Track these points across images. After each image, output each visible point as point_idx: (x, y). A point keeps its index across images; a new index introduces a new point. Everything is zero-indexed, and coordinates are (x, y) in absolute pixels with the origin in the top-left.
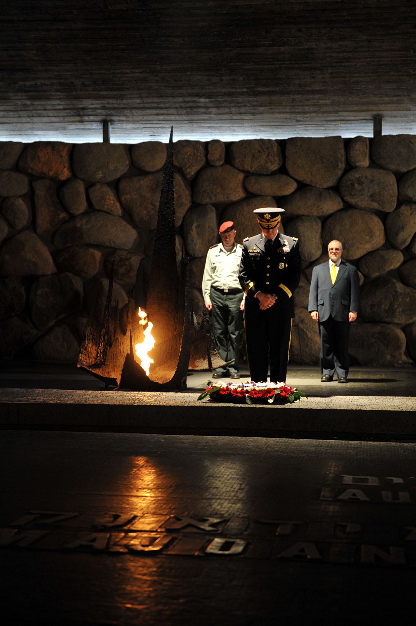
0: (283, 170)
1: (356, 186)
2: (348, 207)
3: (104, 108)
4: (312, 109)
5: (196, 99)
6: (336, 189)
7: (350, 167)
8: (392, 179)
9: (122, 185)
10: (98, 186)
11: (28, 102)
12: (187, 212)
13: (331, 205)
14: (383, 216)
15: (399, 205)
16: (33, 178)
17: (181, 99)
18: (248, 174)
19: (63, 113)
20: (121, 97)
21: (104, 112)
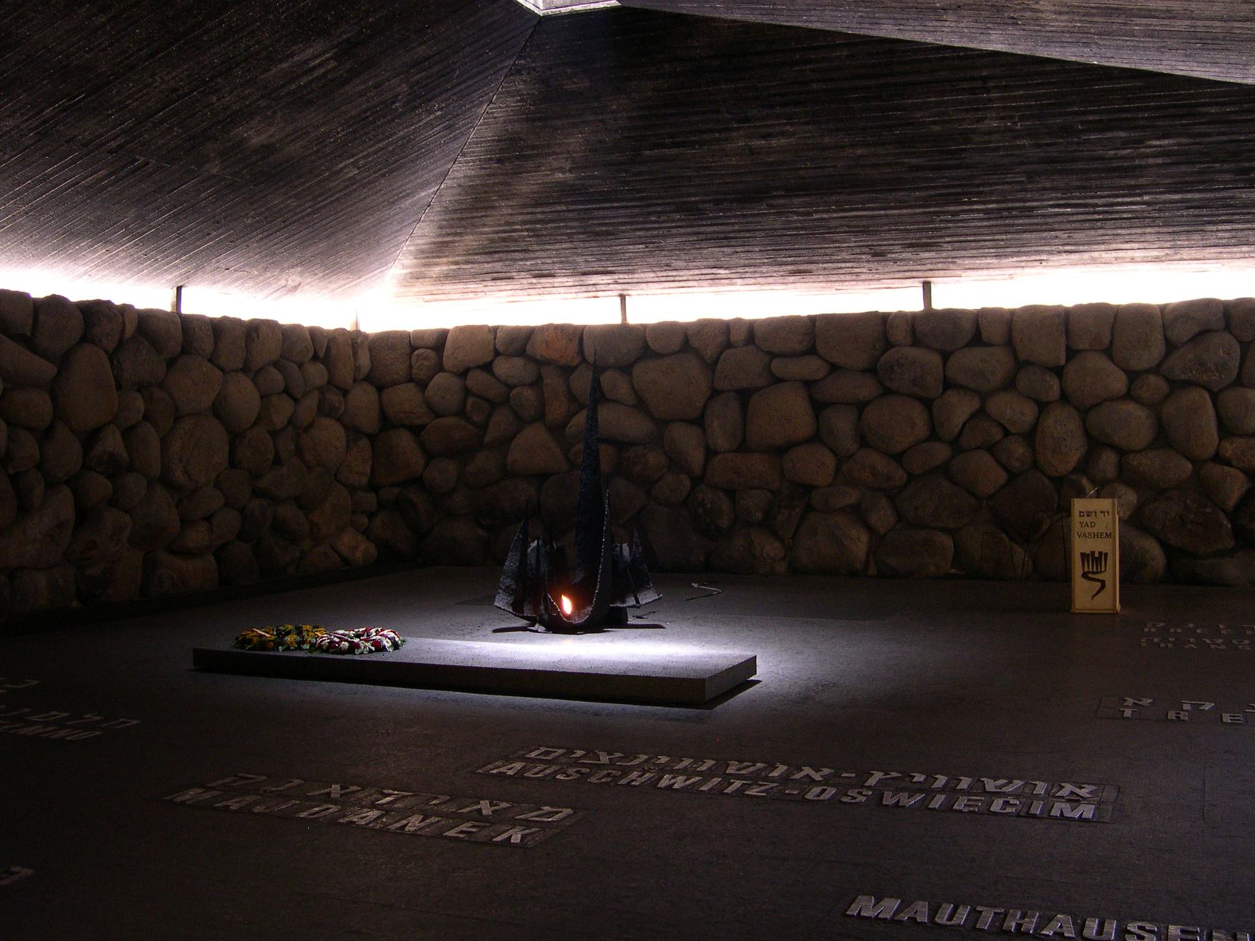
0: (812, 351)
1: (896, 368)
2: (887, 392)
3: (616, 283)
4: (848, 277)
5: (714, 271)
6: (871, 370)
7: (888, 345)
8: (936, 359)
9: (638, 370)
10: (609, 373)
11: (534, 281)
12: (709, 399)
13: (865, 388)
14: (927, 403)
15: (945, 390)
16: (540, 363)
17: (697, 272)
18: (773, 355)
19: (574, 289)
20: (632, 272)
21: (619, 287)
